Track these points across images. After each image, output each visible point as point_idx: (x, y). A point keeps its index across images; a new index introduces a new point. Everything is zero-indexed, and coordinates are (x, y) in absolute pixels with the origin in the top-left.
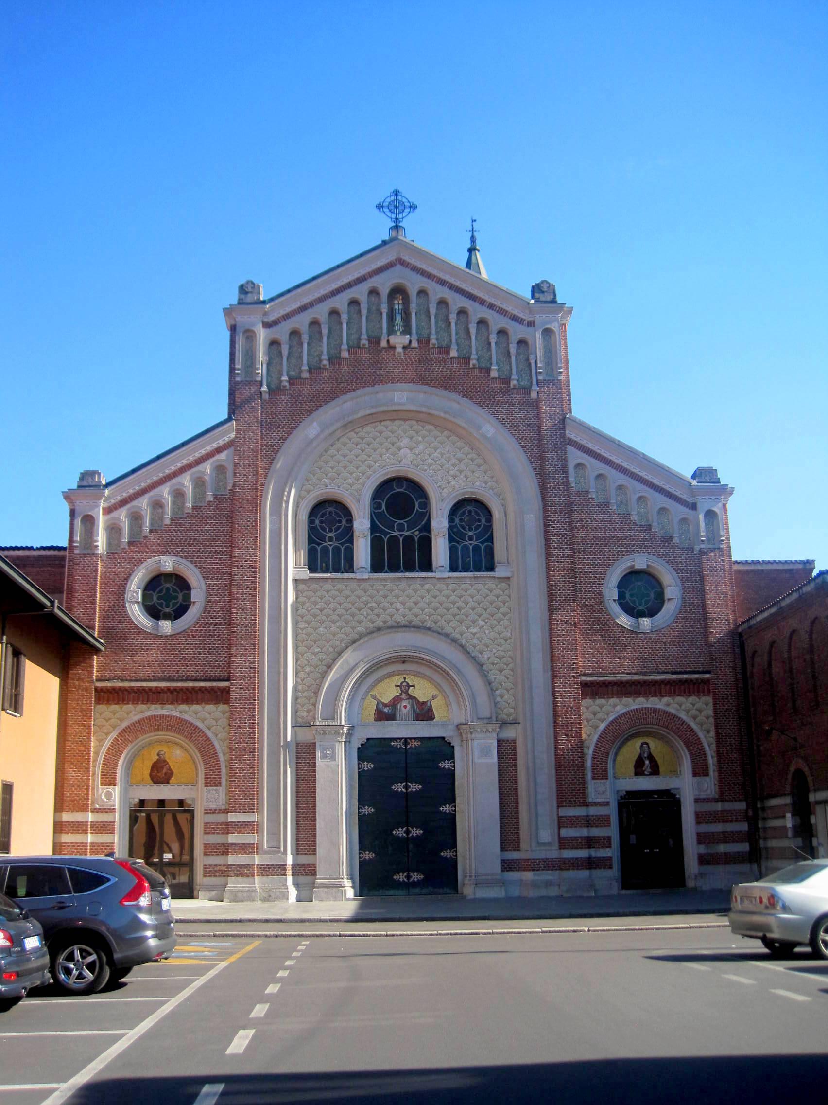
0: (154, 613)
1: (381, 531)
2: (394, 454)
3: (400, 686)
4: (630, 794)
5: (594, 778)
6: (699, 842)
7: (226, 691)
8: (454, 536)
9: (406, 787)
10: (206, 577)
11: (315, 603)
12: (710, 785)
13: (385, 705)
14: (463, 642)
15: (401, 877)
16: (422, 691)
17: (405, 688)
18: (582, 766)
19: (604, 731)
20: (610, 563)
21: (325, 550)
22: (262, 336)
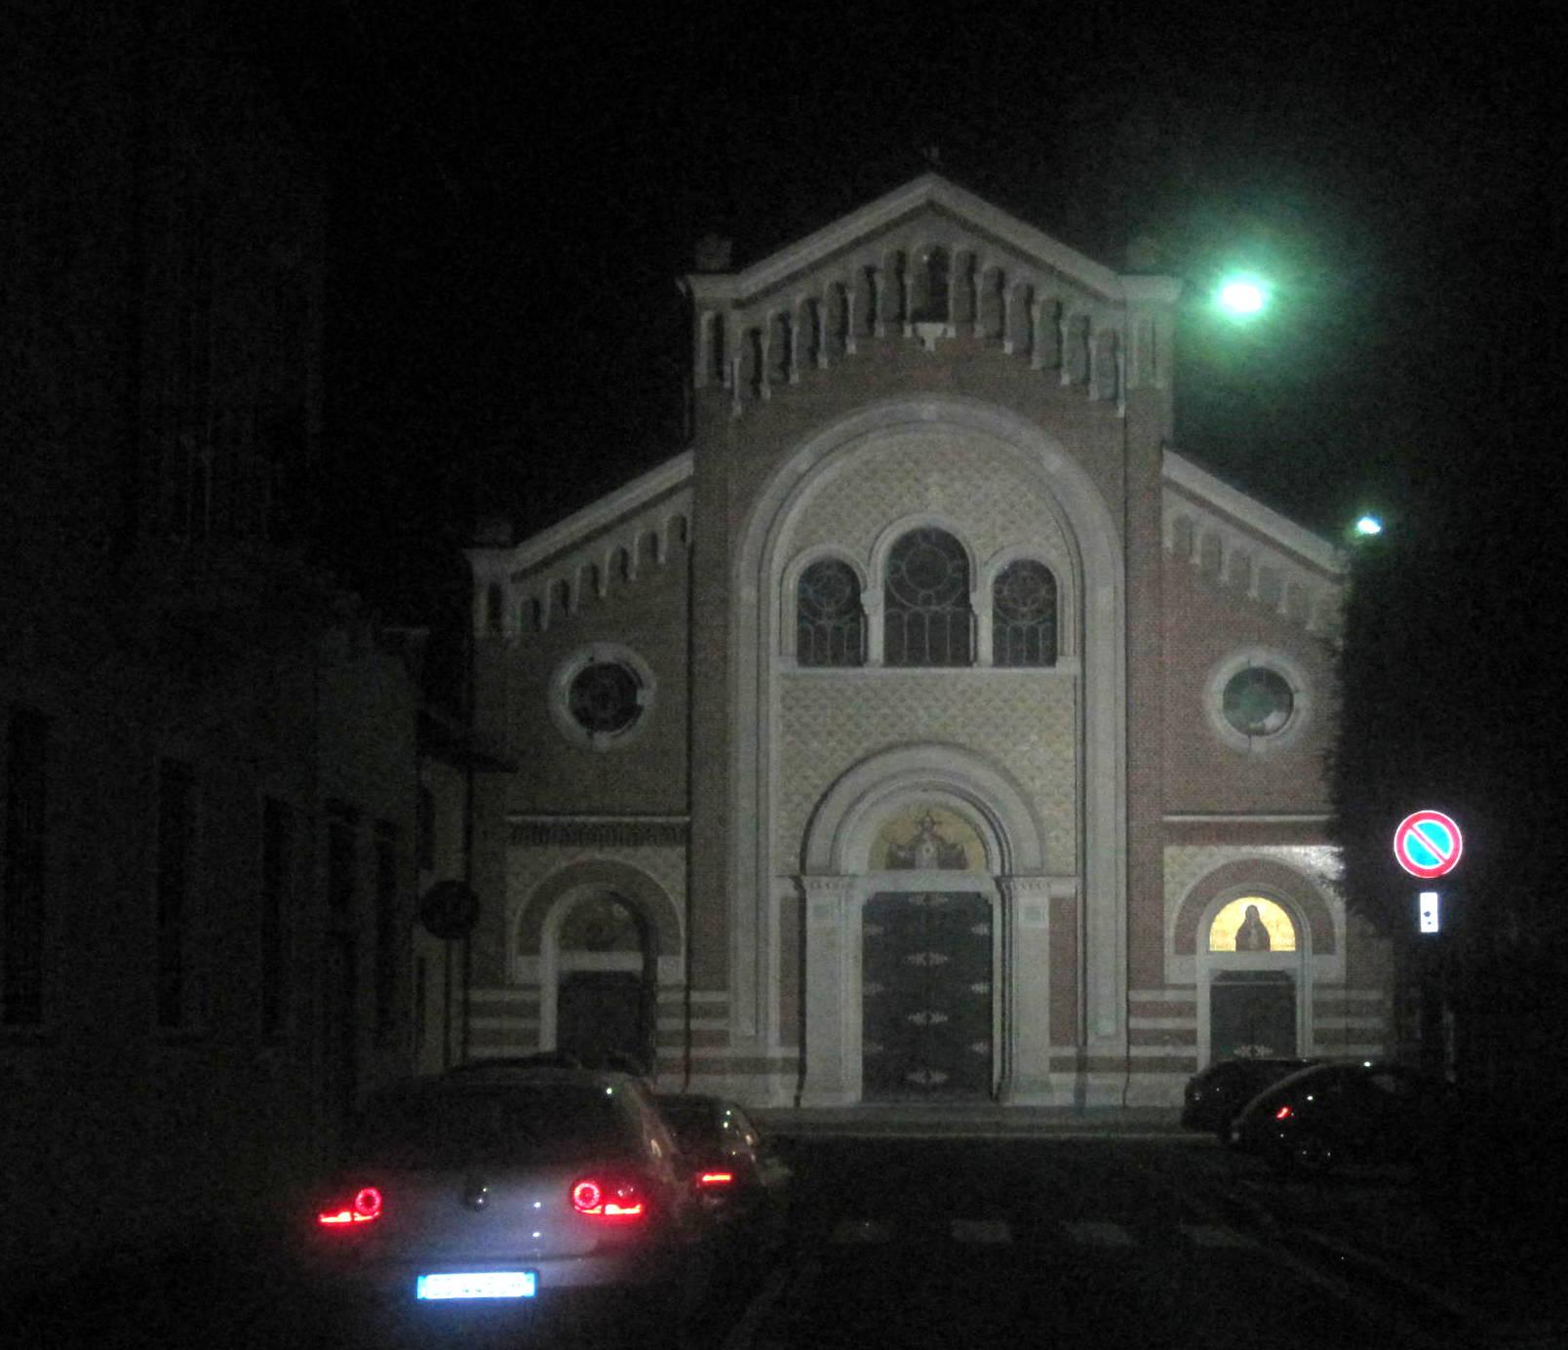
0: (584, 717)
1: (903, 607)
2: (919, 496)
3: (922, 823)
4: (1227, 975)
5: (1178, 952)
6: (1316, 1041)
7: (687, 829)
8: (1003, 612)
9: (927, 959)
10: (656, 668)
11: (807, 708)
12: (1334, 967)
13: (900, 847)
14: (1008, 763)
15: (918, 1077)
16: (951, 831)
17: (927, 825)
18: (1160, 938)
19: (1196, 889)
20: (1215, 658)
21: (820, 630)
22: (737, 326)
